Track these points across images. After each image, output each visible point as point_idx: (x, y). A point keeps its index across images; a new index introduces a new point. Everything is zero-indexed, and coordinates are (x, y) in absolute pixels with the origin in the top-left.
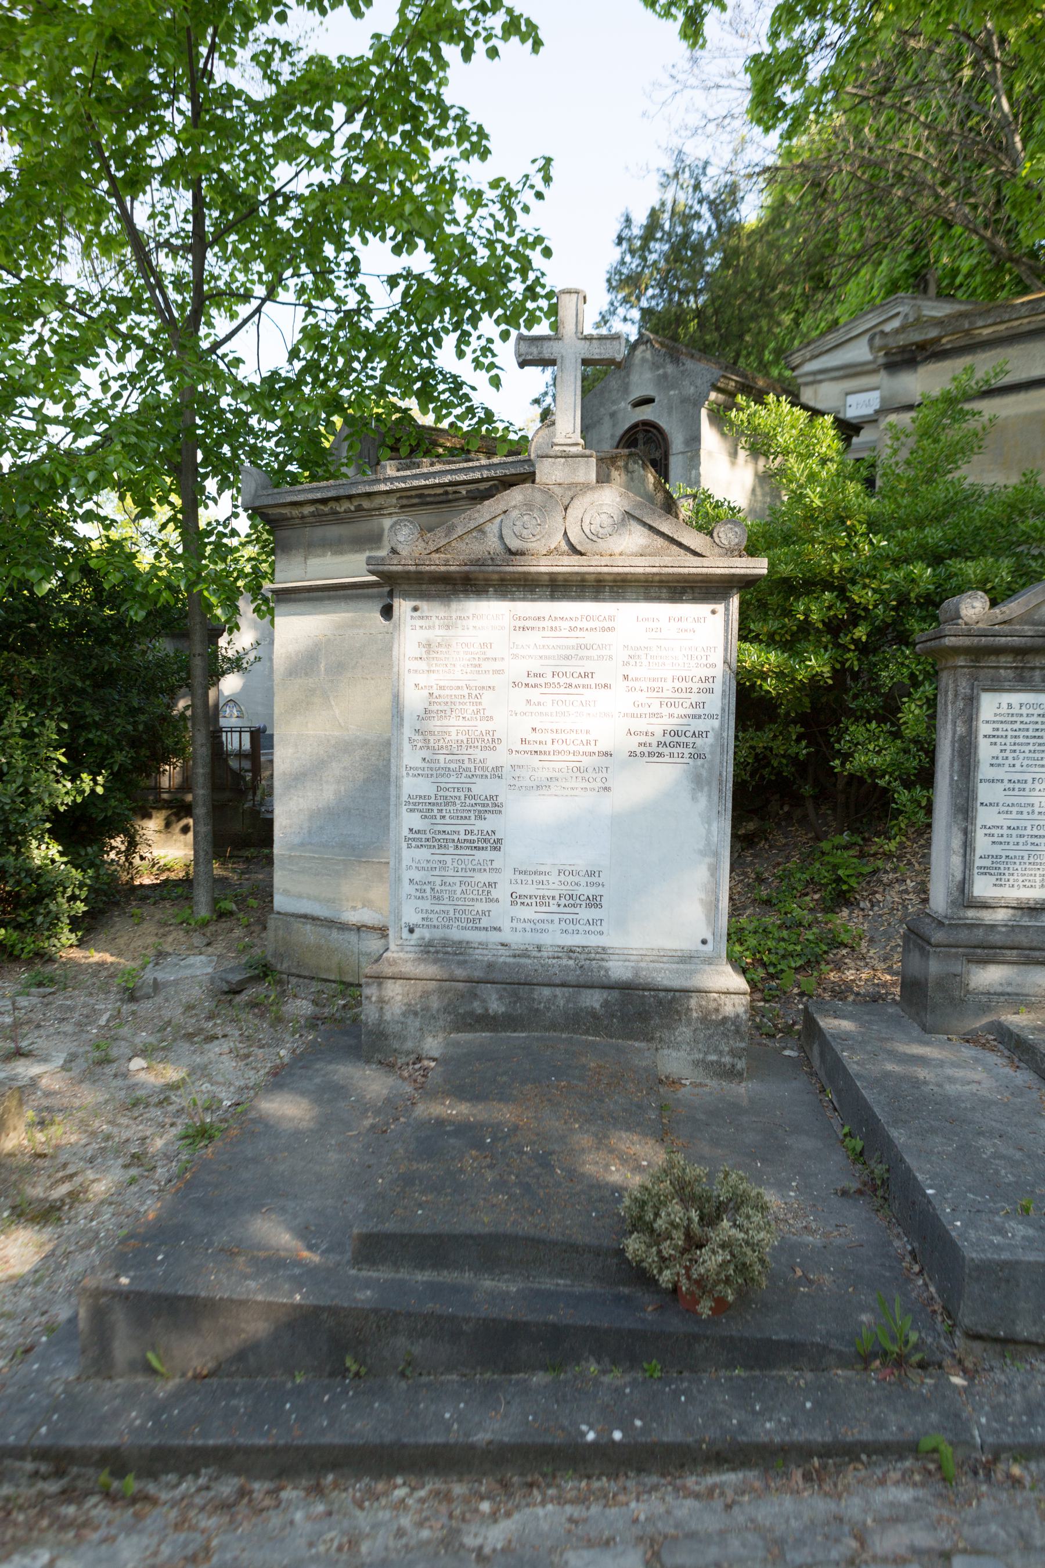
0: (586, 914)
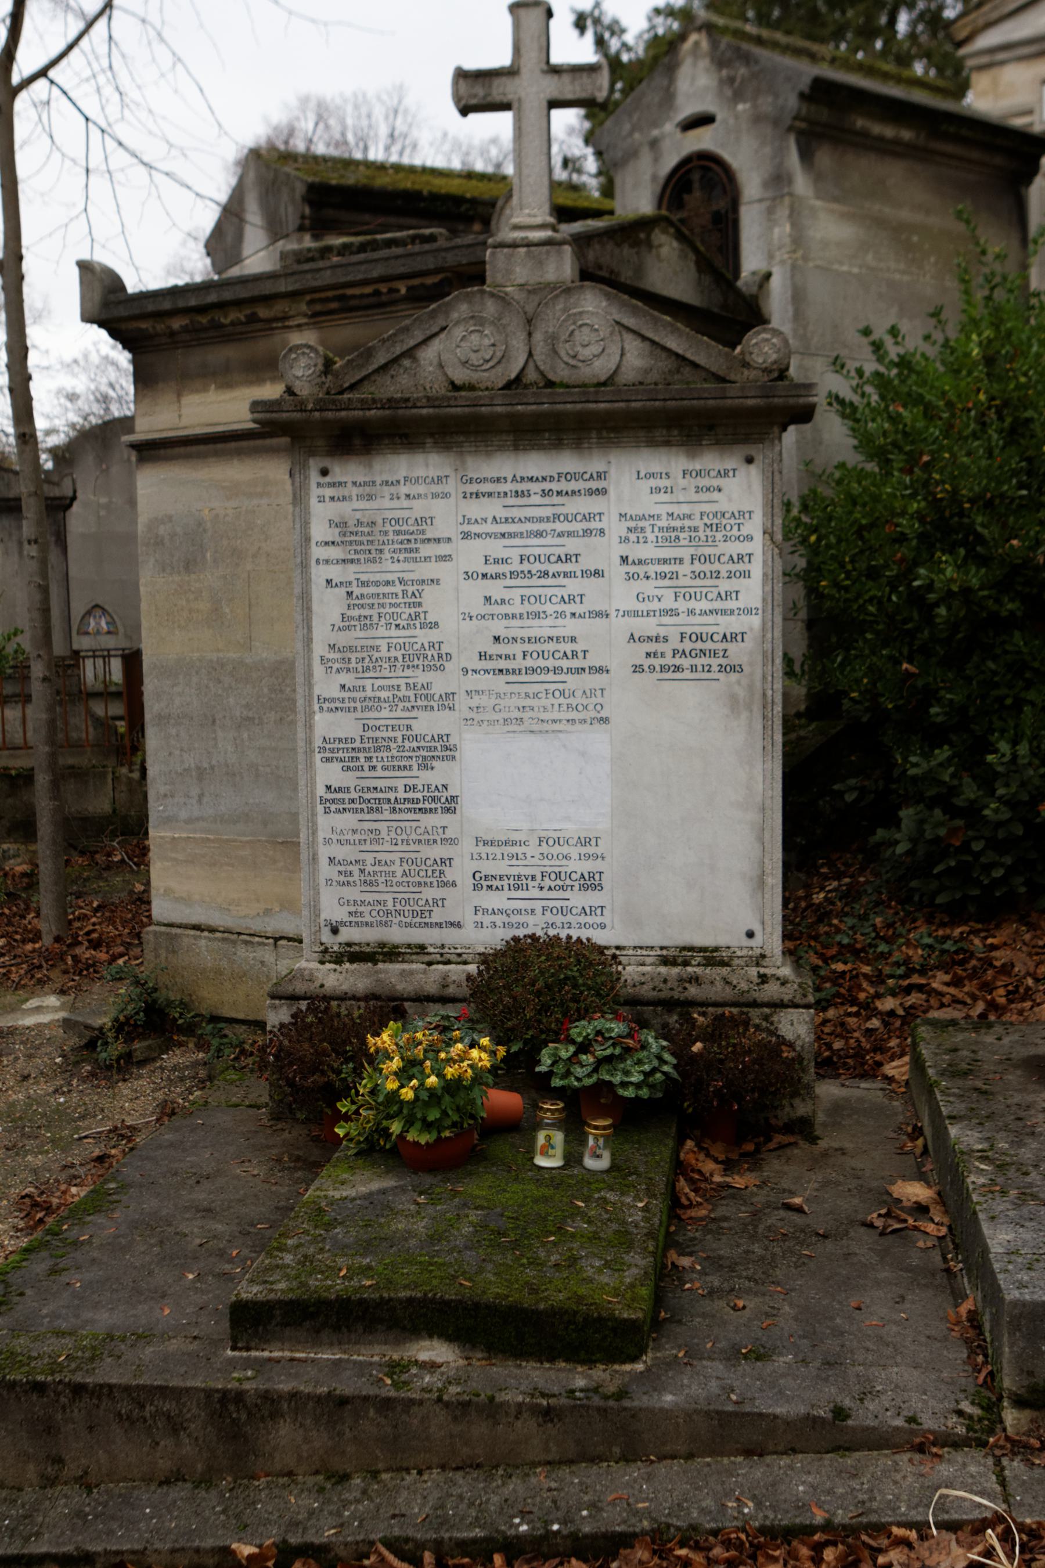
0: (579, 899)
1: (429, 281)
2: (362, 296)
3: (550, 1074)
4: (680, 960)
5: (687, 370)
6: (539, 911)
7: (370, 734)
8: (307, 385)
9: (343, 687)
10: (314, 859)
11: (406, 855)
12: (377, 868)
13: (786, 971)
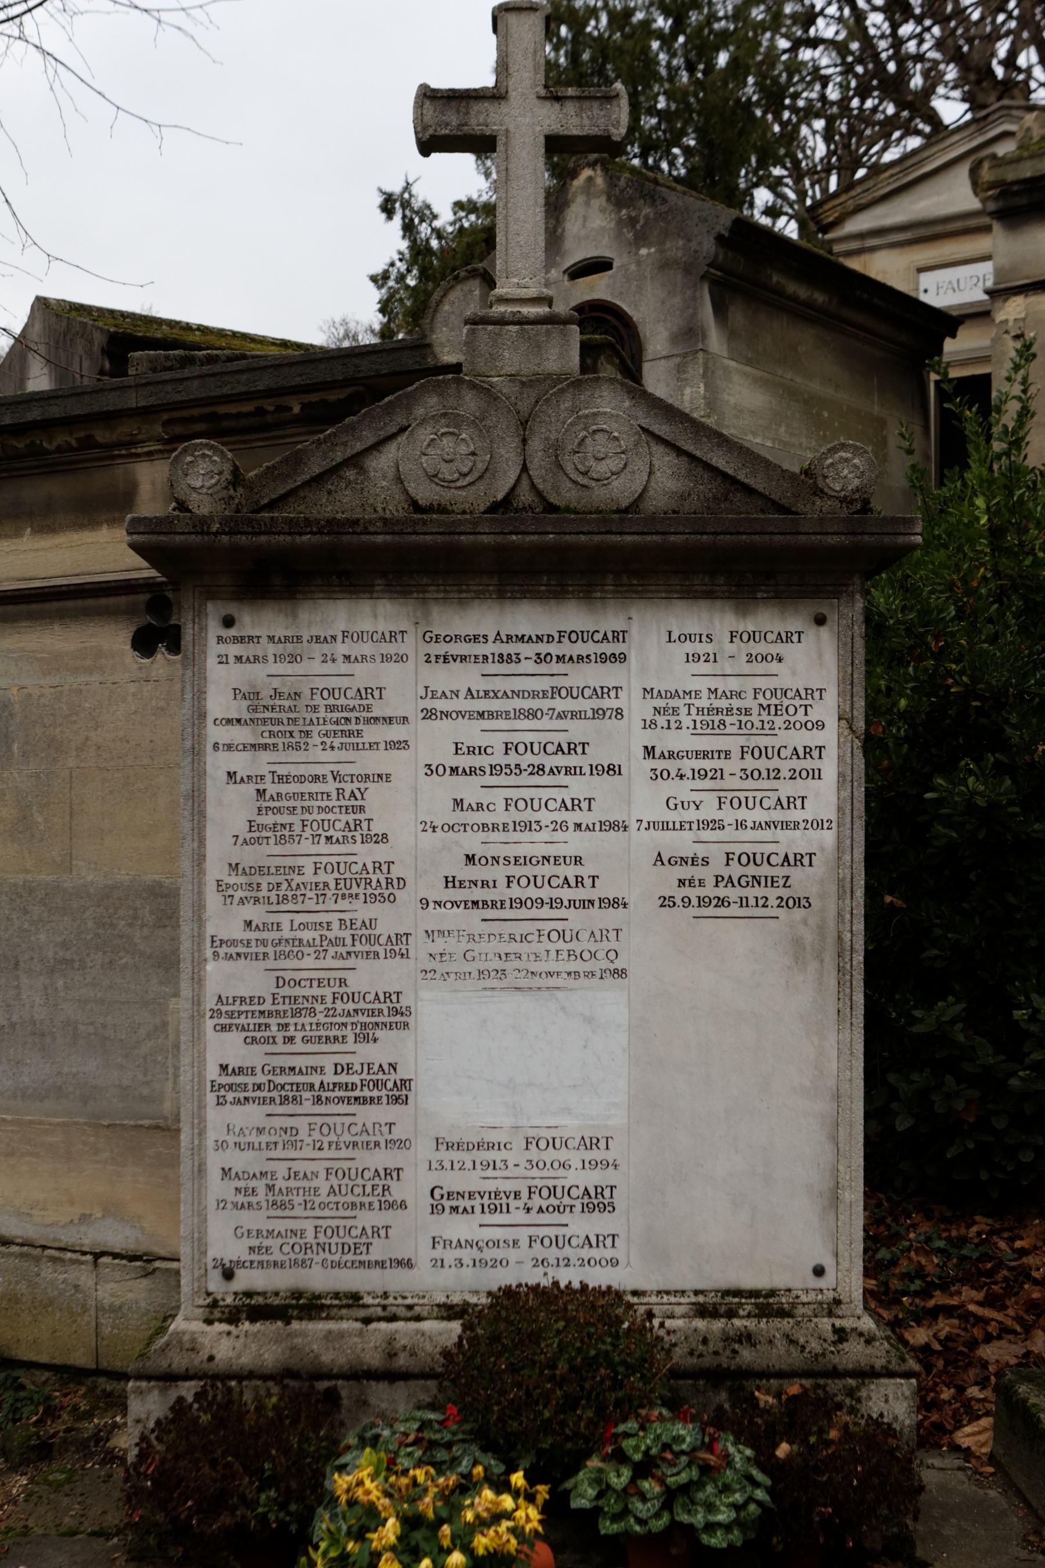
0: (580, 1225)
1: (333, 396)
2: (239, 415)
3: (594, 1514)
4: (723, 1309)
5: (738, 497)
6: (524, 1242)
7: (286, 991)
8: (207, 499)
9: (249, 924)
10: (201, 1170)
11: (336, 1165)
12: (292, 1183)
13: (867, 1323)
